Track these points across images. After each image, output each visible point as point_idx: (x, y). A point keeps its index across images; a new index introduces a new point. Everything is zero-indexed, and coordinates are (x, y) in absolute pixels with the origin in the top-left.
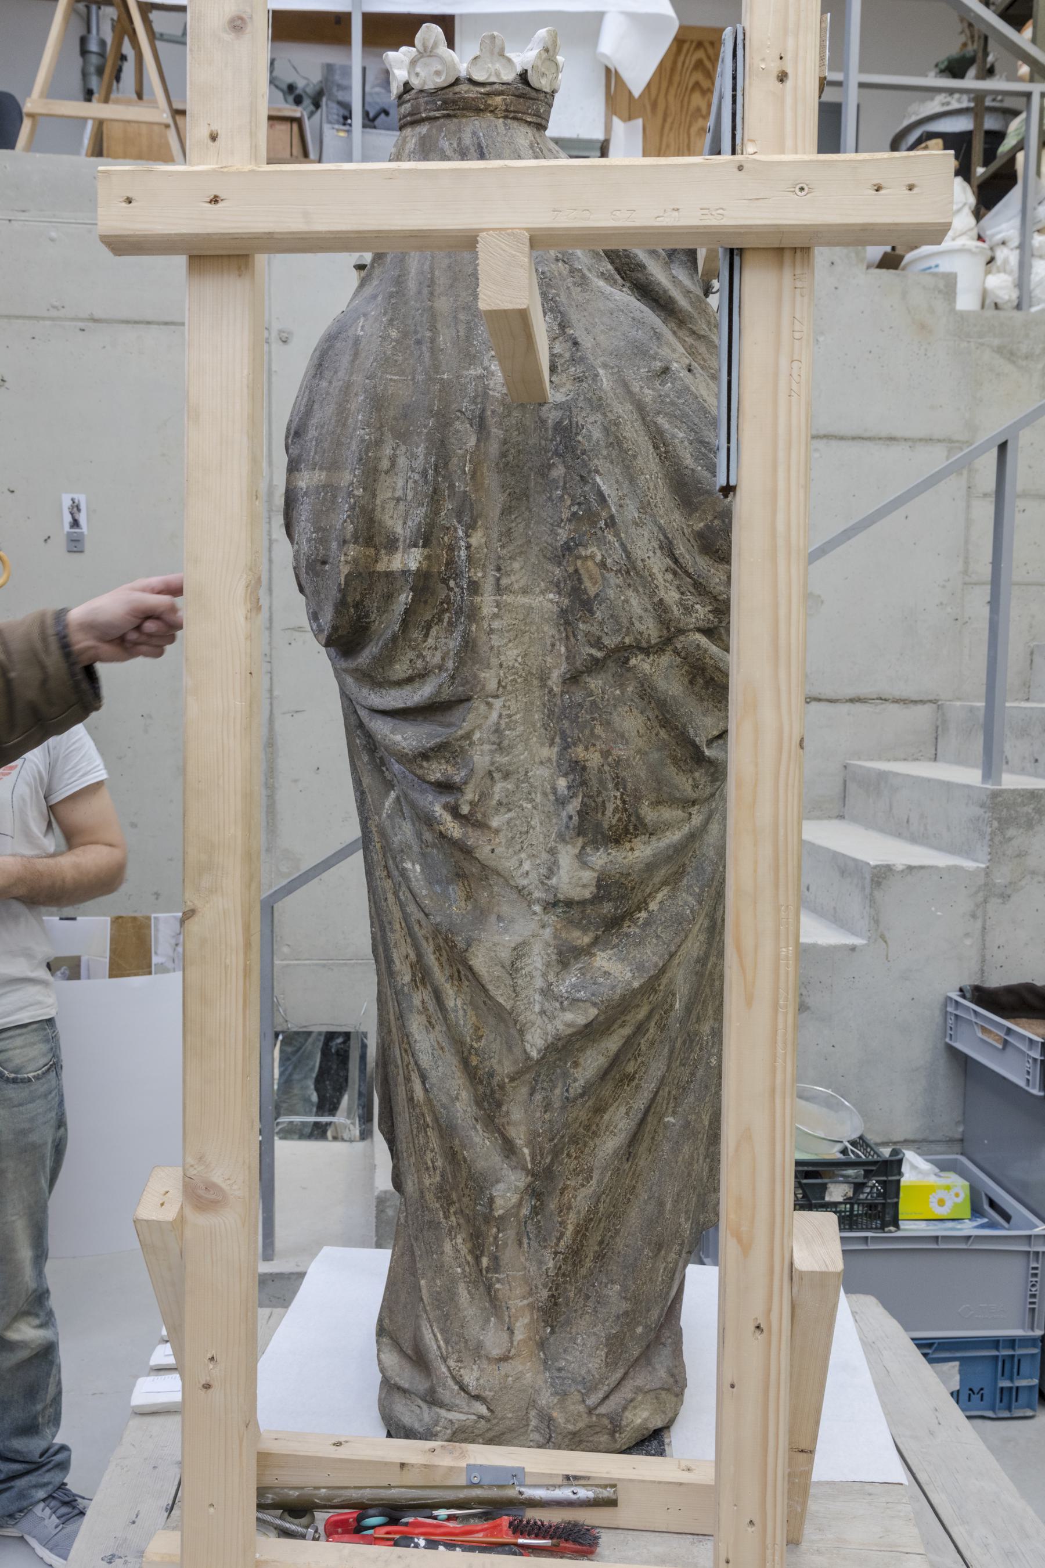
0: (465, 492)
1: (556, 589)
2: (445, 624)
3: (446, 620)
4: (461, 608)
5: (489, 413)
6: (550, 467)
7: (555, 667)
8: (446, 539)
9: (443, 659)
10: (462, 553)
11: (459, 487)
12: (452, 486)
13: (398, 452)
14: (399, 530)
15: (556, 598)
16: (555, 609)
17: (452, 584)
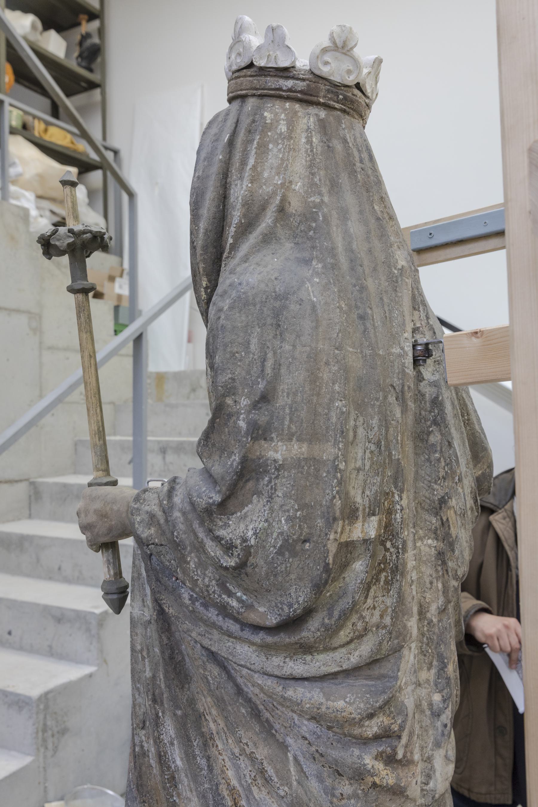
0: (398, 459)
1: (433, 536)
2: (382, 583)
3: (383, 579)
4: (397, 567)
5: (406, 388)
6: (429, 433)
7: (433, 602)
8: (386, 503)
9: (382, 616)
10: (398, 515)
11: (395, 454)
12: (390, 455)
13: (358, 423)
14: (359, 499)
15: (435, 543)
16: (433, 552)
17: (388, 544)
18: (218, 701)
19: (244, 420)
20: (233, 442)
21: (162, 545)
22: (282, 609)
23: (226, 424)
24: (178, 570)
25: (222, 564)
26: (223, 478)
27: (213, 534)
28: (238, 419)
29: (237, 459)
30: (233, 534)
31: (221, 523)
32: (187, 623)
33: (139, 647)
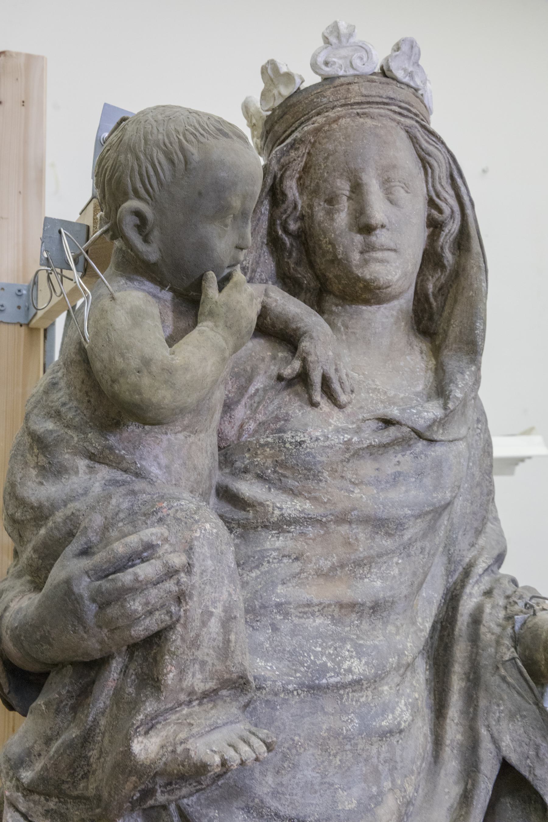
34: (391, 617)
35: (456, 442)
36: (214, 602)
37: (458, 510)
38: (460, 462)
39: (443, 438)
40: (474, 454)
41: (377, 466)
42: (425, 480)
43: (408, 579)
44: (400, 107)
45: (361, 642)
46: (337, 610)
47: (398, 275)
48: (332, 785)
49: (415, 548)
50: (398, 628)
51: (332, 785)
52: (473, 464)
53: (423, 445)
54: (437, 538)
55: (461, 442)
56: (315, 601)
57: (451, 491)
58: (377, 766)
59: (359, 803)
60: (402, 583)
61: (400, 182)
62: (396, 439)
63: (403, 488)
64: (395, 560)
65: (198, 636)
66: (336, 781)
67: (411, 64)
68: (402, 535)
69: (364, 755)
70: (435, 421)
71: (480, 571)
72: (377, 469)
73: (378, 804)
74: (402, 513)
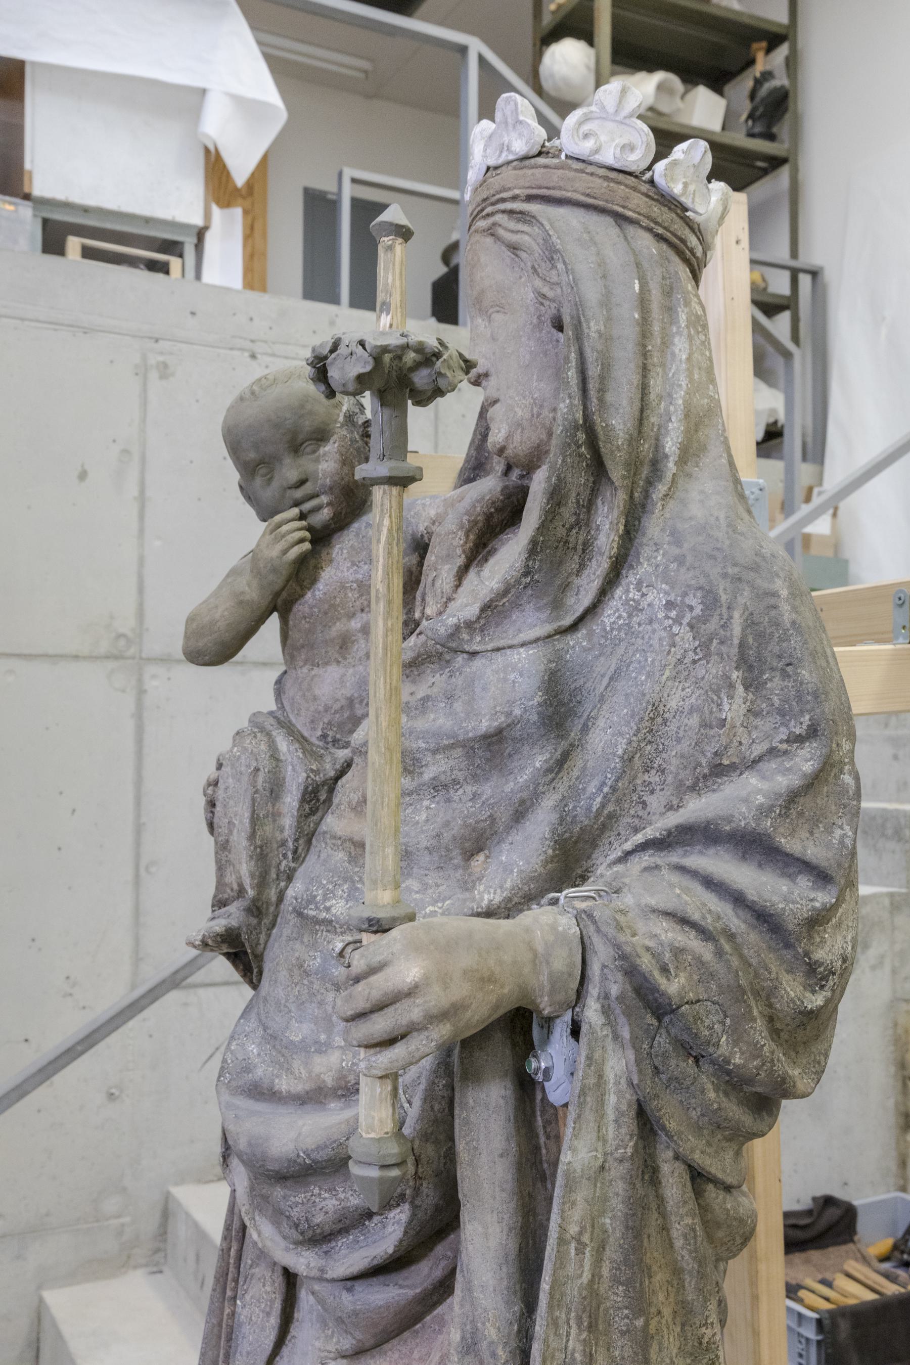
18: (700, 1266)
19: (850, 774)
20: (833, 808)
21: (698, 1001)
22: (819, 1063)
23: (826, 780)
24: (724, 1039)
25: (806, 1007)
26: (839, 865)
27: (810, 959)
28: (841, 772)
29: (850, 833)
30: (833, 954)
31: (818, 940)
32: (690, 1137)
33: (573, 1229)
34: (415, 870)
35: (508, 652)
36: (236, 815)
37: (600, 749)
38: (505, 680)
39: (478, 648)
40: (653, 661)
41: (413, 689)
42: (455, 705)
43: (434, 828)
44: (493, 204)
45: (359, 886)
46: (352, 847)
47: (503, 431)
48: (290, 1011)
49: (459, 793)
50: (425, 887)
51: (290, 1011)
52: (649, 676)
53: (463, 658)
54: (512, 784)
55: (522, 650)
56: (339, 833)
57: (490, 719)
58: (331, 1016)
59: (303, 1041)
60: (422, 832)
61: (492, 307)
62: (419, 656)
63: (432, 716)
64: (426, 803)
65: (227, 841)
66: (293, 1009)
67: (510, 128)
68: (421, 773)
69: (319, 997)
70: (457, 628)
71: (628, 846)
72: (412, 694)
73: (319, 1052)
74: (415, 746)
